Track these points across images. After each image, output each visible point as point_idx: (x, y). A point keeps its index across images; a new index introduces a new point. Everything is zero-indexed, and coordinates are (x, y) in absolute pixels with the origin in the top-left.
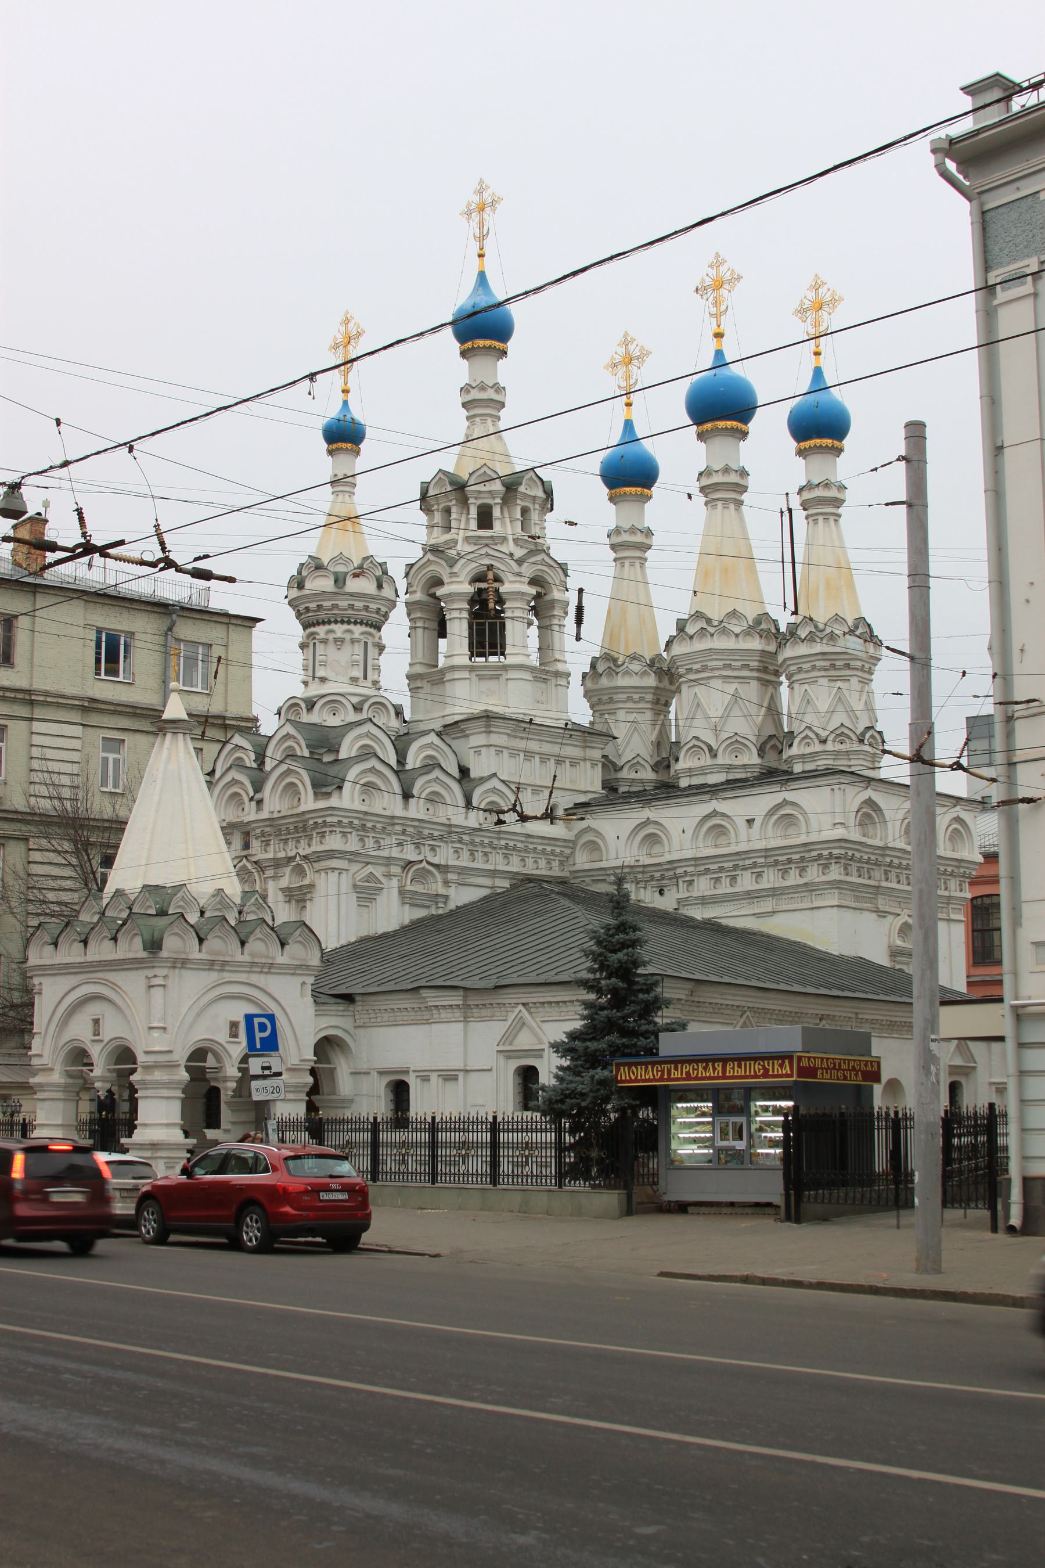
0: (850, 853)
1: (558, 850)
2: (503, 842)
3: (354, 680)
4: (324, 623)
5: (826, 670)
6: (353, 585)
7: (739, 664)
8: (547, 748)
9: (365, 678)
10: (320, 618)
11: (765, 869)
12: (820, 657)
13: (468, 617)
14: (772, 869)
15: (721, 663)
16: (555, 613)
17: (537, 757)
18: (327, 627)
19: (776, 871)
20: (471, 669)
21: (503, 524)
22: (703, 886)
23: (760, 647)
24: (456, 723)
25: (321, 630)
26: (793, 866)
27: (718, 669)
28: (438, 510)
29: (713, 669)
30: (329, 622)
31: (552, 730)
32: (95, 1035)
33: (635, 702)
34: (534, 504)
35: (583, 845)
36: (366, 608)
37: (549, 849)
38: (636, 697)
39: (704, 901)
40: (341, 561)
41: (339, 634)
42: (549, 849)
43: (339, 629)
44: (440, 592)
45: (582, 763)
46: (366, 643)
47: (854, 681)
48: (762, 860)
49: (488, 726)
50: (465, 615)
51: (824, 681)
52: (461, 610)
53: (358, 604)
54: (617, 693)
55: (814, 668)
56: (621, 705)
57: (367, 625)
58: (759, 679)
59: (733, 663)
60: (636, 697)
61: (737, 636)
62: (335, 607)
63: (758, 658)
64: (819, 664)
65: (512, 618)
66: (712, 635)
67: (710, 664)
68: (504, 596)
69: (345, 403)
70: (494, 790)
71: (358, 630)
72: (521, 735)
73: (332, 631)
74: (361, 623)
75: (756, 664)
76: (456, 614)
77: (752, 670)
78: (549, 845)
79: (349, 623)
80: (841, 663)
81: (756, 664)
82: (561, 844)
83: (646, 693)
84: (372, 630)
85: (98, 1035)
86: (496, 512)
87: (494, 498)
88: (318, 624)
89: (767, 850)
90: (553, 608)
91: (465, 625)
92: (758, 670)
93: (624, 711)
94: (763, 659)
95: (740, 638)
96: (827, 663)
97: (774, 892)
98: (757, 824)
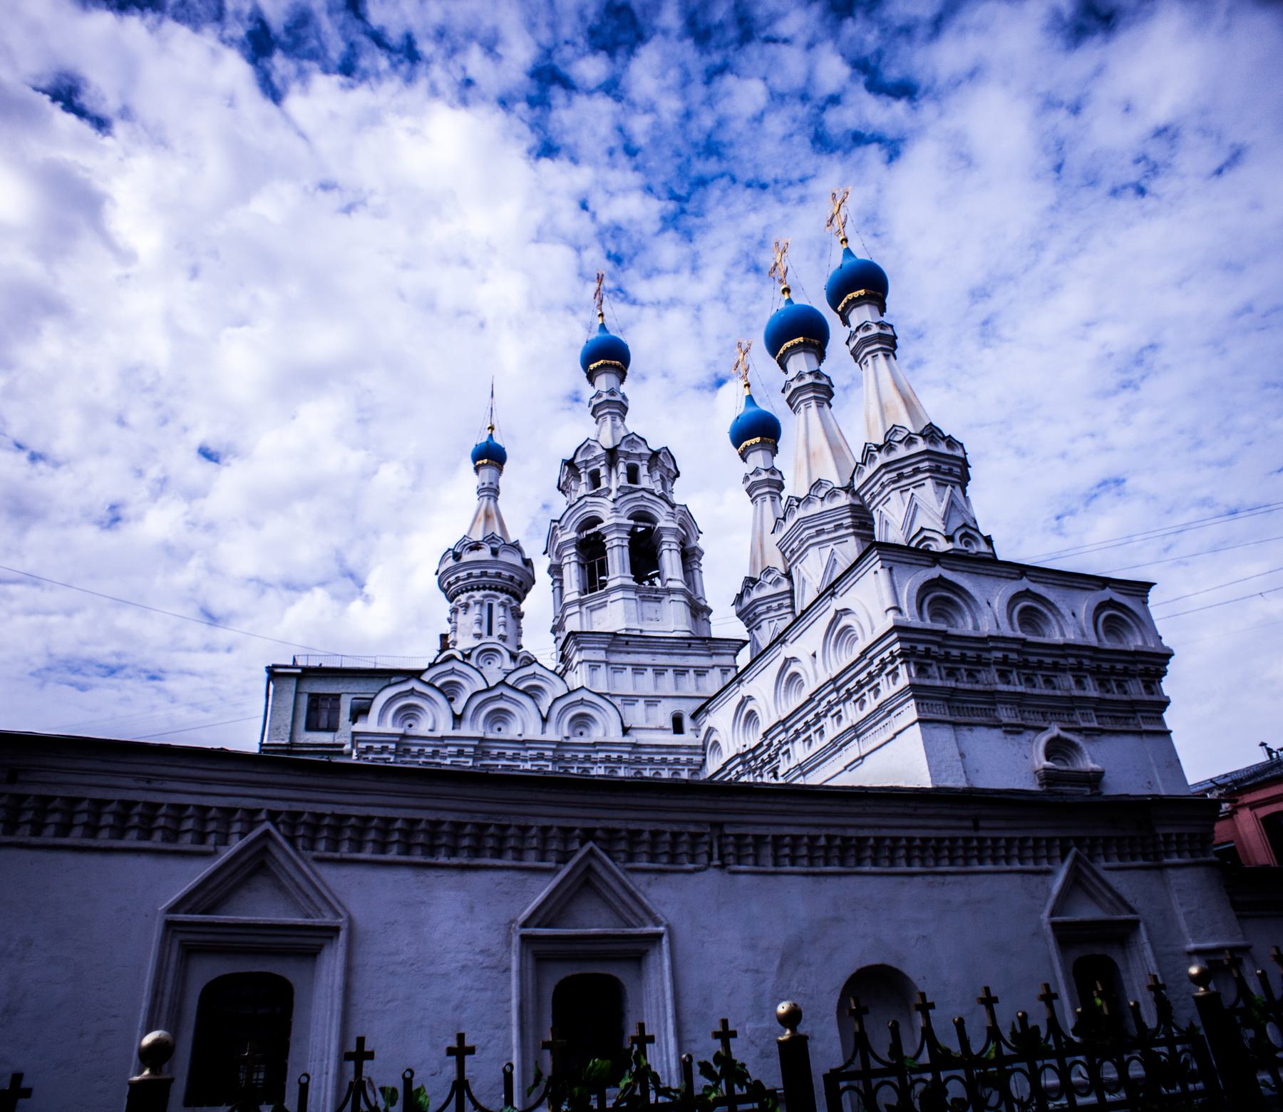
0: (921, 647)
1: (683, 758)
2: (602, 755)
3: (478, 636)
5: (894, 482)
6: (468, 557)
7: (832, 525)
8: (662, 660)
9: (490, 633)
11: (841, 706)
12: (883, 471)
13: (575, 559)
14: (848, 704)
15: (813, 530)
16: (663, 539)
17: (650, 670)
19: (853, 704)
20: (581, 603)
21: (609, 480)
22: (800, 752)
23: (847, 502)
26: (865, 690)
27: (812, 537)
29: (808, 539)
31: (662, 640)
33: (776, 610)
34: (641, 461)
35: (711, 750)
36: (484, 574)
37: (671, 758)
38: (775, 605)
39: (803, 768)
42: (671, 758)
45: (710, 670)
46: (490, 606)
47: (929, 483)
48: (834, 695)
49: (577, 643)
51: (895, 496)
53: (476, 572)
54: (757, 607)
55: (883, 486)
56: (763, 617)
57: (490, 589)
58: (854, 534)
59: (825, 527)
60: (775, 605)
62: (458, 579)
63: (849, 514)
64: (884, 479)
65: (612, 548)
66: (798, 507)
67: (803, 536)
68: (603, 532)
69: (491, 436)
70: (582, 702)
71: (478, 595)
72: (625, 649)
73: (459, 601)
74: (484, 588)
75: (849, 520)
77: (847, 528)
78: (670, 754)
80: (910, 469)
81: (849, 520)
82: (686, 751)
83: (783, 599)
84: (498, 594)
86: (603, 472)
87: (599, 462)
89: (834, 680)
90: (661, 537)
91: (574, 566)
92: (853, 526)
93: (766, 622)
94: (856, 514)
95: (826, 501)
96: (894, 474)
97: (856, 731)
98: (819, 655)
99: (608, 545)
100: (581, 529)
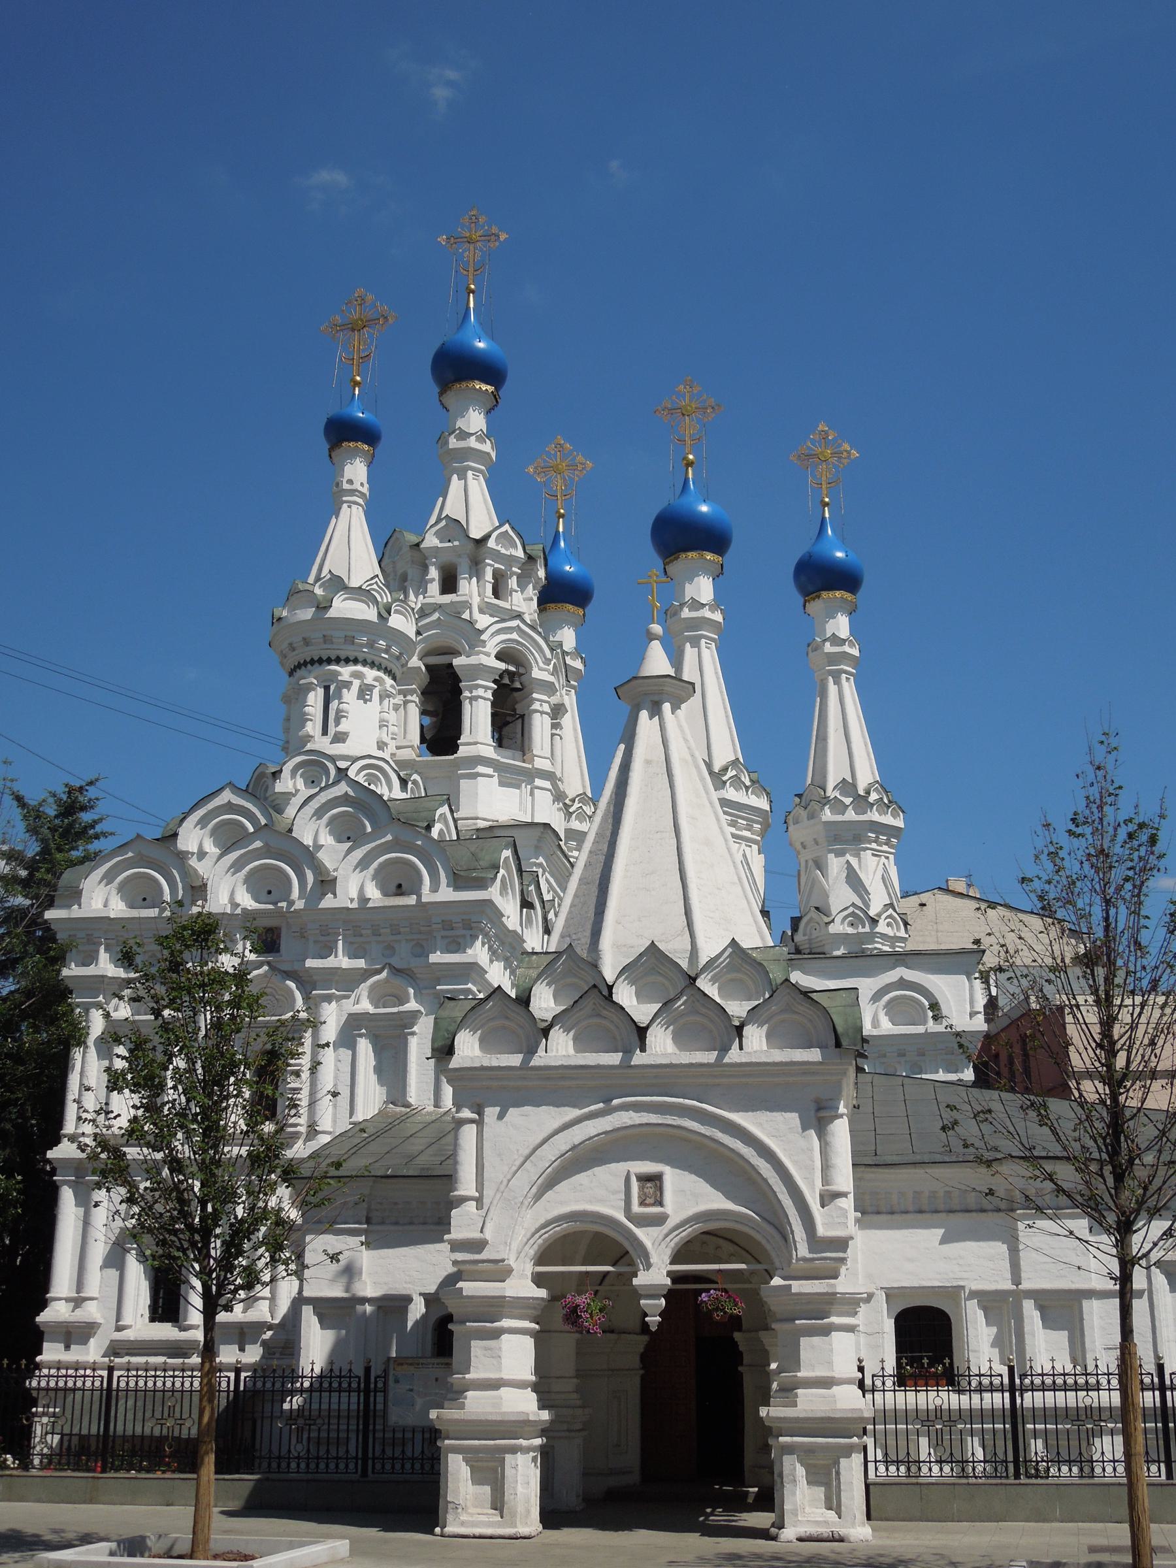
4: (347, 661)
10: (343, 655)
18: (352, 668)
24: (491, 827)
25: (345, 672)
28: (434, 564)
30: (356, 661)
32: (642, 1203)
40: (375, 586)
41: (369, 680)
43: (370, 674)
44: (457, 662)
50: (489, 695)
52: (486, 688)
61: (747, 788)
71: (389, 682)
76: (480, 692)
79: (379, 668)
85: (660, 1203)
86: (513, 583)
88: (338, 661)
99: (536, 706)
100: (499, 657)
